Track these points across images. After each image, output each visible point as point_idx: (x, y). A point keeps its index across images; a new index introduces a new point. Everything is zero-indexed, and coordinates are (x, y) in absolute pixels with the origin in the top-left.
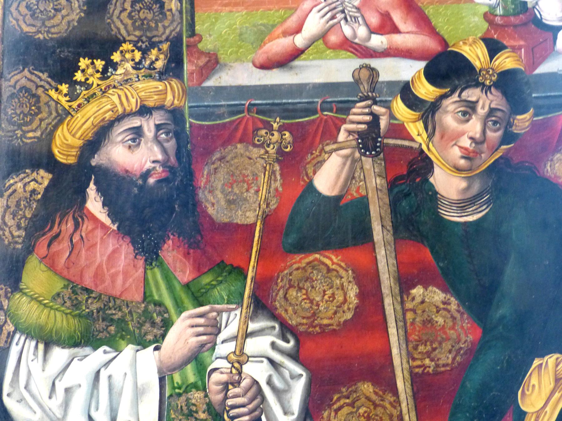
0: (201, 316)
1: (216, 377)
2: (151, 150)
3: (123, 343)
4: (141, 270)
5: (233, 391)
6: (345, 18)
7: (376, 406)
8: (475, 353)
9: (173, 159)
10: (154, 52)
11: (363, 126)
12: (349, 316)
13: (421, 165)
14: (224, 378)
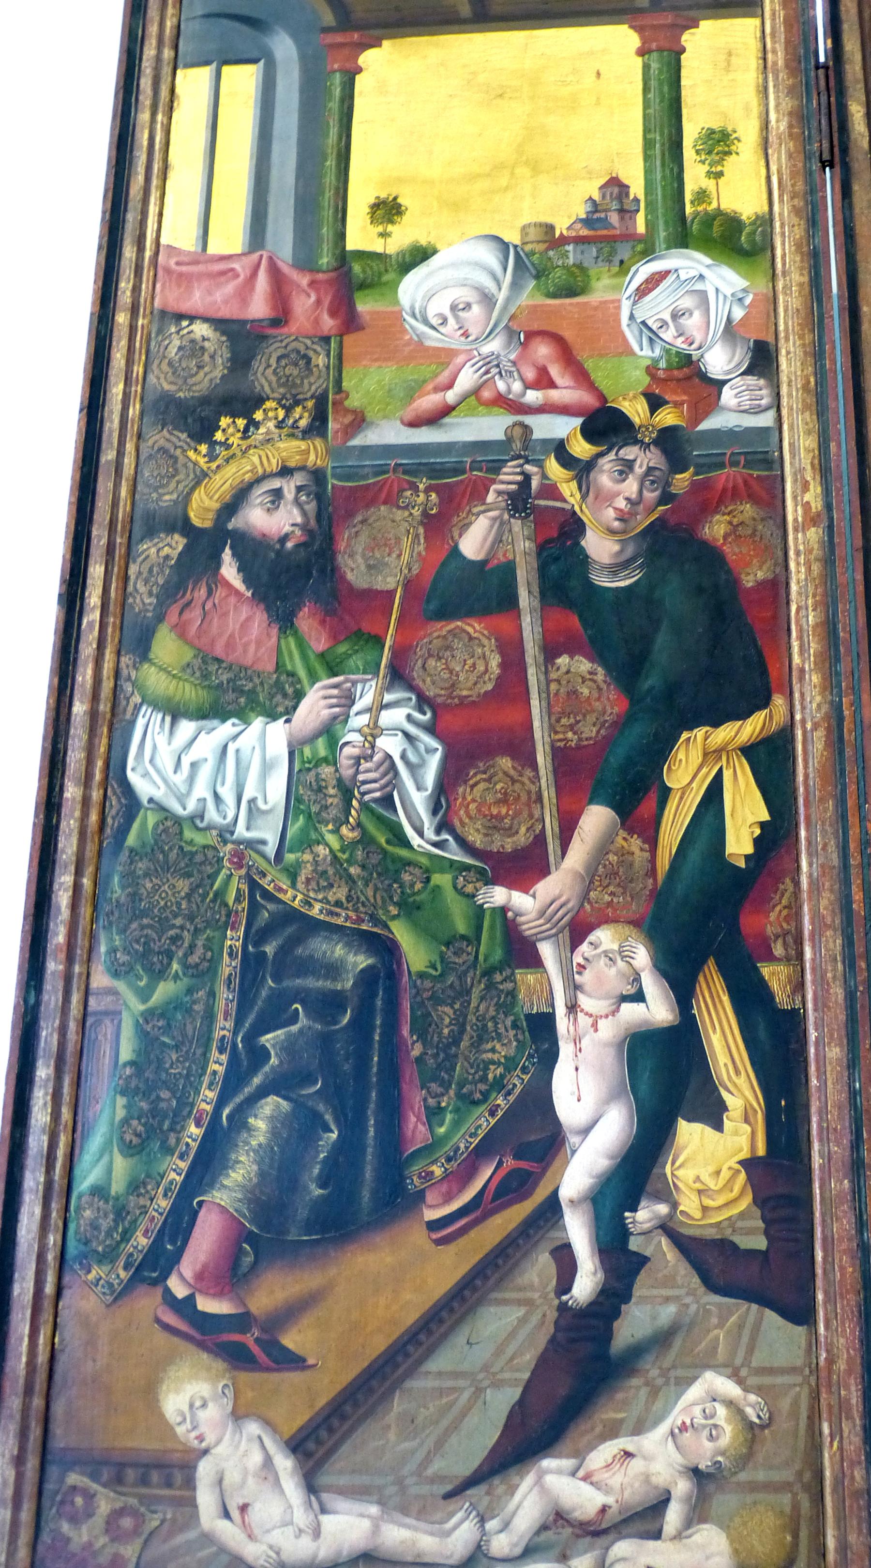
0: (335, 686)
1: (347, 751)
2: (290, 513)
3: (252, 715)
4: (274, 639)
5: (364, 765)
6: (500, 373)
7: (514, 781)
8: (621, 725)
9: (313, 522)
10: (299, 410)
11: (514, 487)
12: (489, 687)
13: (573, 527)
14: (356, 751)
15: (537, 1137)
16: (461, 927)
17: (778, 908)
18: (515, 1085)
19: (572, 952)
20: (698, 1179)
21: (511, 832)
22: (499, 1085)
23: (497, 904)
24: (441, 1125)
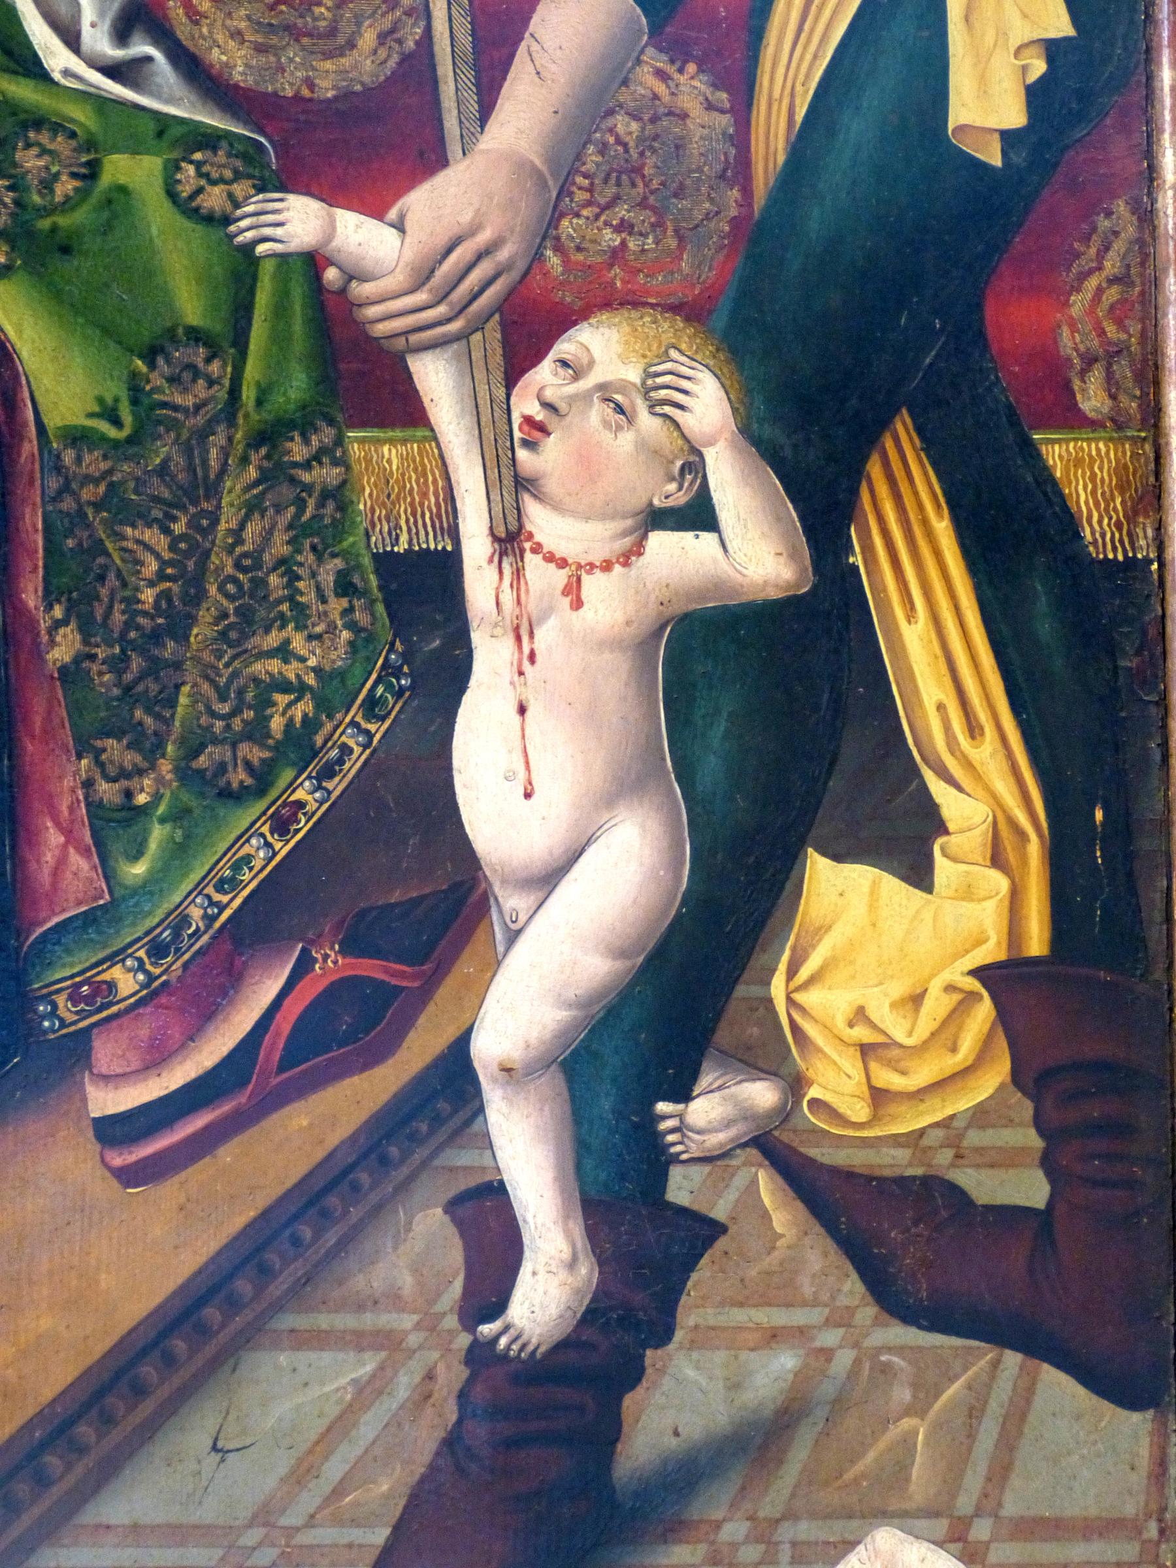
15: (416, 899)
16: (192, 306)
17: (1093, 282)
18: (346, 750)
19: (511, 381)
20: (860, 1015)
21: (333, 42)
22: (300, 747)
23: (294, 246)
24: (136, 855)
